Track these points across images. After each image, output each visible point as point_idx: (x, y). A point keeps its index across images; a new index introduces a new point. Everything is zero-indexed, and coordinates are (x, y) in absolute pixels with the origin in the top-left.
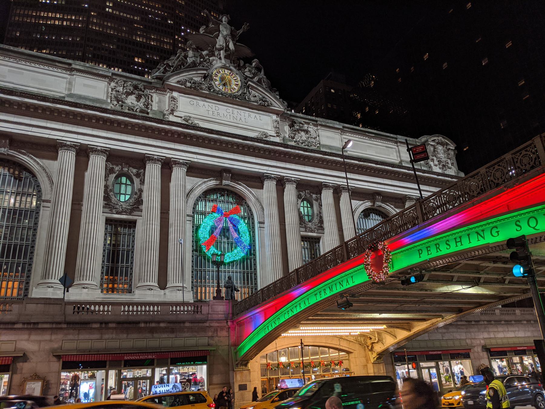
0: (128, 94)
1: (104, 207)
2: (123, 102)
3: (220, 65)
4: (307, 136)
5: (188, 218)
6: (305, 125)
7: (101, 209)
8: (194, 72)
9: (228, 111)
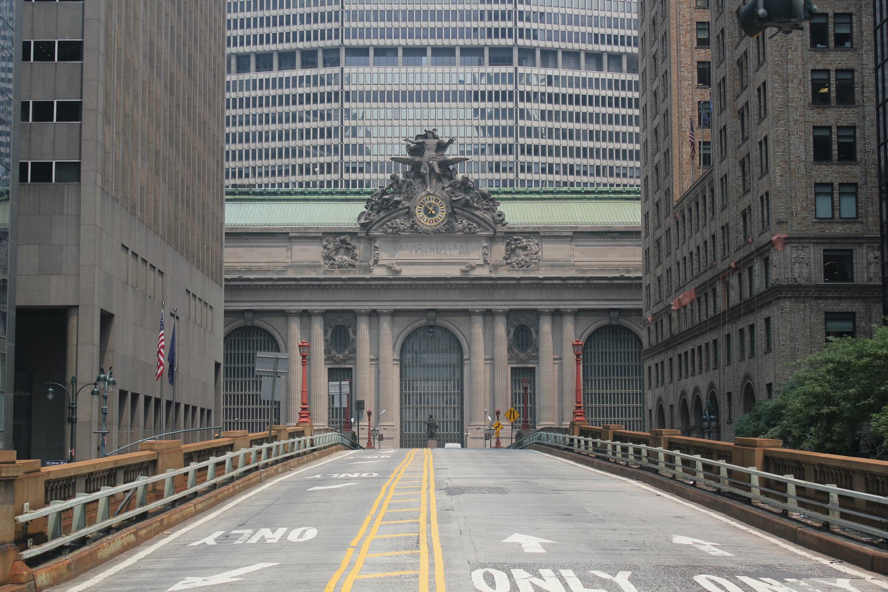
0: (337, 250)
1: (325, 360)
2: (334, 260)
3: (424, 193)
4: (527, 253)
5: (395, 363)
6: (524, 240)
7: (323, 362)
8: (396, 214)
9: (432, 246)
